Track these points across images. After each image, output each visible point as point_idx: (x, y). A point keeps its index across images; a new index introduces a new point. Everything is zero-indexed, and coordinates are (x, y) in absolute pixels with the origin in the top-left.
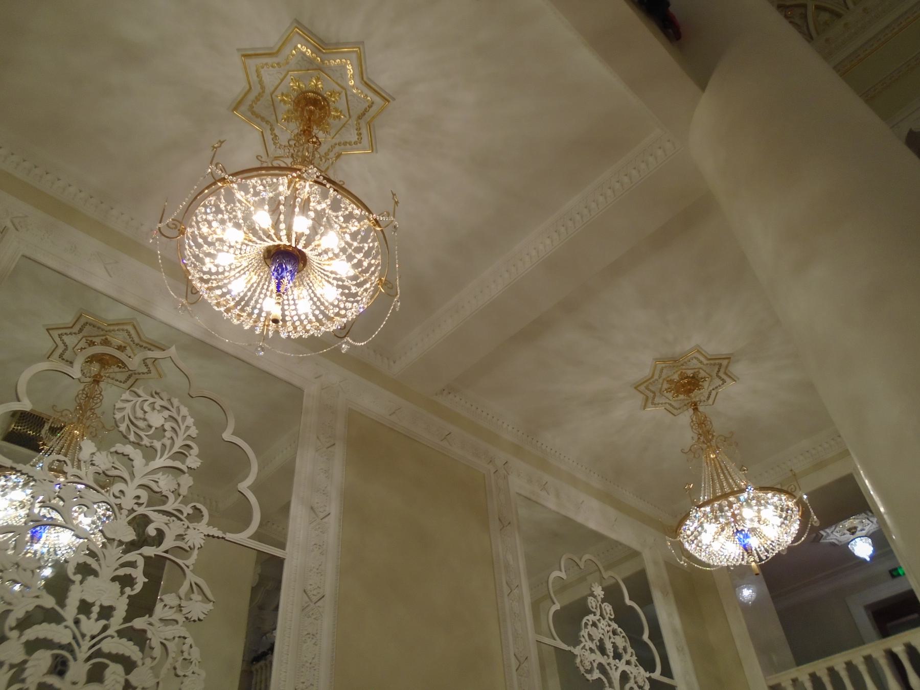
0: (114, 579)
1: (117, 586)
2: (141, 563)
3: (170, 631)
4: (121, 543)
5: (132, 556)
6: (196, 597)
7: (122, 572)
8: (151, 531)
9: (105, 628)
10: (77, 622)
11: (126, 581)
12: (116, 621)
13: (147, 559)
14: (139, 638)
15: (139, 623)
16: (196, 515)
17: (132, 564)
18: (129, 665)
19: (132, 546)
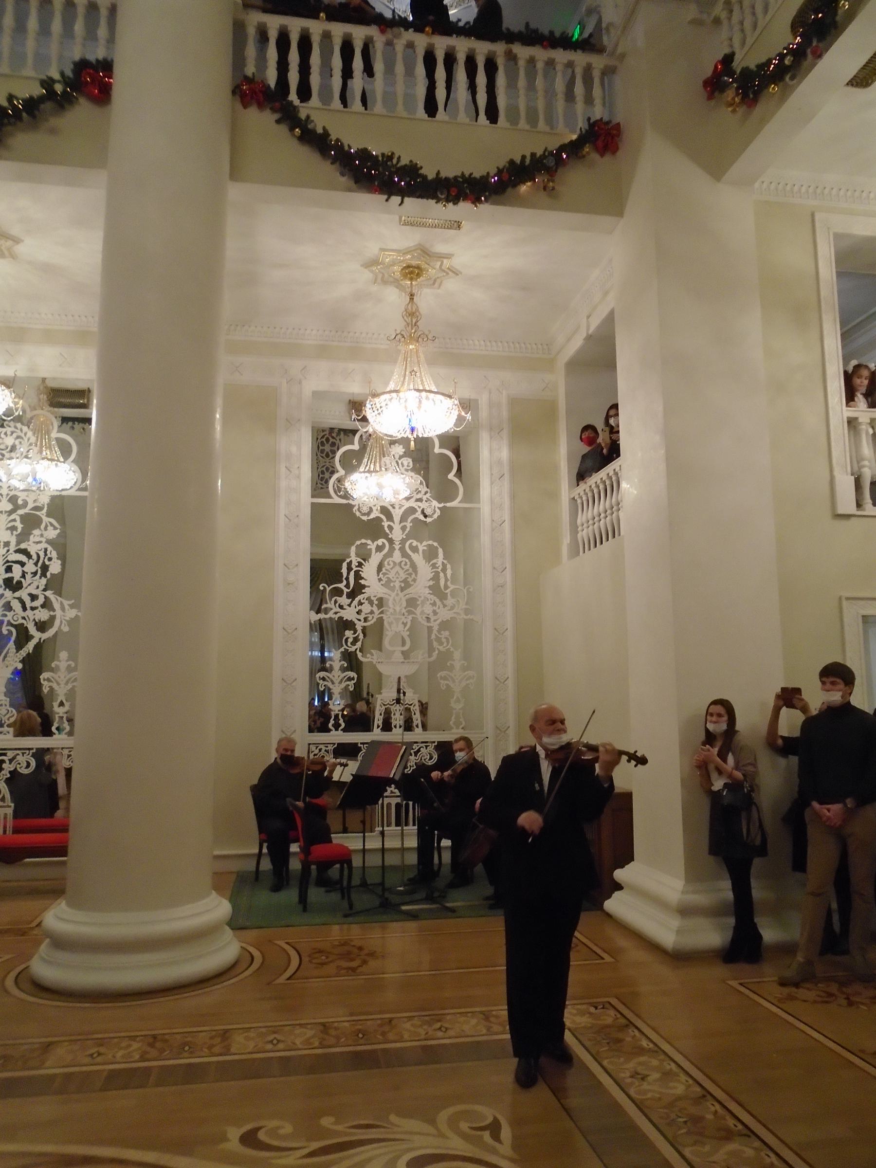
0: (7, 529)
1: (9, 532)
2: (18, 519)
3: (39, 546)
4: (6, 512)
5: (13, 517)
6: (50, 528)
7: (9, 525)
8: (20, 502)
9: (8, 551)
11: (13, 529)
12: (13, 547)
13: (21, 516)
14: (25, 552)
15: (23, 546)
17: (14, 520)
18: (22, 564)
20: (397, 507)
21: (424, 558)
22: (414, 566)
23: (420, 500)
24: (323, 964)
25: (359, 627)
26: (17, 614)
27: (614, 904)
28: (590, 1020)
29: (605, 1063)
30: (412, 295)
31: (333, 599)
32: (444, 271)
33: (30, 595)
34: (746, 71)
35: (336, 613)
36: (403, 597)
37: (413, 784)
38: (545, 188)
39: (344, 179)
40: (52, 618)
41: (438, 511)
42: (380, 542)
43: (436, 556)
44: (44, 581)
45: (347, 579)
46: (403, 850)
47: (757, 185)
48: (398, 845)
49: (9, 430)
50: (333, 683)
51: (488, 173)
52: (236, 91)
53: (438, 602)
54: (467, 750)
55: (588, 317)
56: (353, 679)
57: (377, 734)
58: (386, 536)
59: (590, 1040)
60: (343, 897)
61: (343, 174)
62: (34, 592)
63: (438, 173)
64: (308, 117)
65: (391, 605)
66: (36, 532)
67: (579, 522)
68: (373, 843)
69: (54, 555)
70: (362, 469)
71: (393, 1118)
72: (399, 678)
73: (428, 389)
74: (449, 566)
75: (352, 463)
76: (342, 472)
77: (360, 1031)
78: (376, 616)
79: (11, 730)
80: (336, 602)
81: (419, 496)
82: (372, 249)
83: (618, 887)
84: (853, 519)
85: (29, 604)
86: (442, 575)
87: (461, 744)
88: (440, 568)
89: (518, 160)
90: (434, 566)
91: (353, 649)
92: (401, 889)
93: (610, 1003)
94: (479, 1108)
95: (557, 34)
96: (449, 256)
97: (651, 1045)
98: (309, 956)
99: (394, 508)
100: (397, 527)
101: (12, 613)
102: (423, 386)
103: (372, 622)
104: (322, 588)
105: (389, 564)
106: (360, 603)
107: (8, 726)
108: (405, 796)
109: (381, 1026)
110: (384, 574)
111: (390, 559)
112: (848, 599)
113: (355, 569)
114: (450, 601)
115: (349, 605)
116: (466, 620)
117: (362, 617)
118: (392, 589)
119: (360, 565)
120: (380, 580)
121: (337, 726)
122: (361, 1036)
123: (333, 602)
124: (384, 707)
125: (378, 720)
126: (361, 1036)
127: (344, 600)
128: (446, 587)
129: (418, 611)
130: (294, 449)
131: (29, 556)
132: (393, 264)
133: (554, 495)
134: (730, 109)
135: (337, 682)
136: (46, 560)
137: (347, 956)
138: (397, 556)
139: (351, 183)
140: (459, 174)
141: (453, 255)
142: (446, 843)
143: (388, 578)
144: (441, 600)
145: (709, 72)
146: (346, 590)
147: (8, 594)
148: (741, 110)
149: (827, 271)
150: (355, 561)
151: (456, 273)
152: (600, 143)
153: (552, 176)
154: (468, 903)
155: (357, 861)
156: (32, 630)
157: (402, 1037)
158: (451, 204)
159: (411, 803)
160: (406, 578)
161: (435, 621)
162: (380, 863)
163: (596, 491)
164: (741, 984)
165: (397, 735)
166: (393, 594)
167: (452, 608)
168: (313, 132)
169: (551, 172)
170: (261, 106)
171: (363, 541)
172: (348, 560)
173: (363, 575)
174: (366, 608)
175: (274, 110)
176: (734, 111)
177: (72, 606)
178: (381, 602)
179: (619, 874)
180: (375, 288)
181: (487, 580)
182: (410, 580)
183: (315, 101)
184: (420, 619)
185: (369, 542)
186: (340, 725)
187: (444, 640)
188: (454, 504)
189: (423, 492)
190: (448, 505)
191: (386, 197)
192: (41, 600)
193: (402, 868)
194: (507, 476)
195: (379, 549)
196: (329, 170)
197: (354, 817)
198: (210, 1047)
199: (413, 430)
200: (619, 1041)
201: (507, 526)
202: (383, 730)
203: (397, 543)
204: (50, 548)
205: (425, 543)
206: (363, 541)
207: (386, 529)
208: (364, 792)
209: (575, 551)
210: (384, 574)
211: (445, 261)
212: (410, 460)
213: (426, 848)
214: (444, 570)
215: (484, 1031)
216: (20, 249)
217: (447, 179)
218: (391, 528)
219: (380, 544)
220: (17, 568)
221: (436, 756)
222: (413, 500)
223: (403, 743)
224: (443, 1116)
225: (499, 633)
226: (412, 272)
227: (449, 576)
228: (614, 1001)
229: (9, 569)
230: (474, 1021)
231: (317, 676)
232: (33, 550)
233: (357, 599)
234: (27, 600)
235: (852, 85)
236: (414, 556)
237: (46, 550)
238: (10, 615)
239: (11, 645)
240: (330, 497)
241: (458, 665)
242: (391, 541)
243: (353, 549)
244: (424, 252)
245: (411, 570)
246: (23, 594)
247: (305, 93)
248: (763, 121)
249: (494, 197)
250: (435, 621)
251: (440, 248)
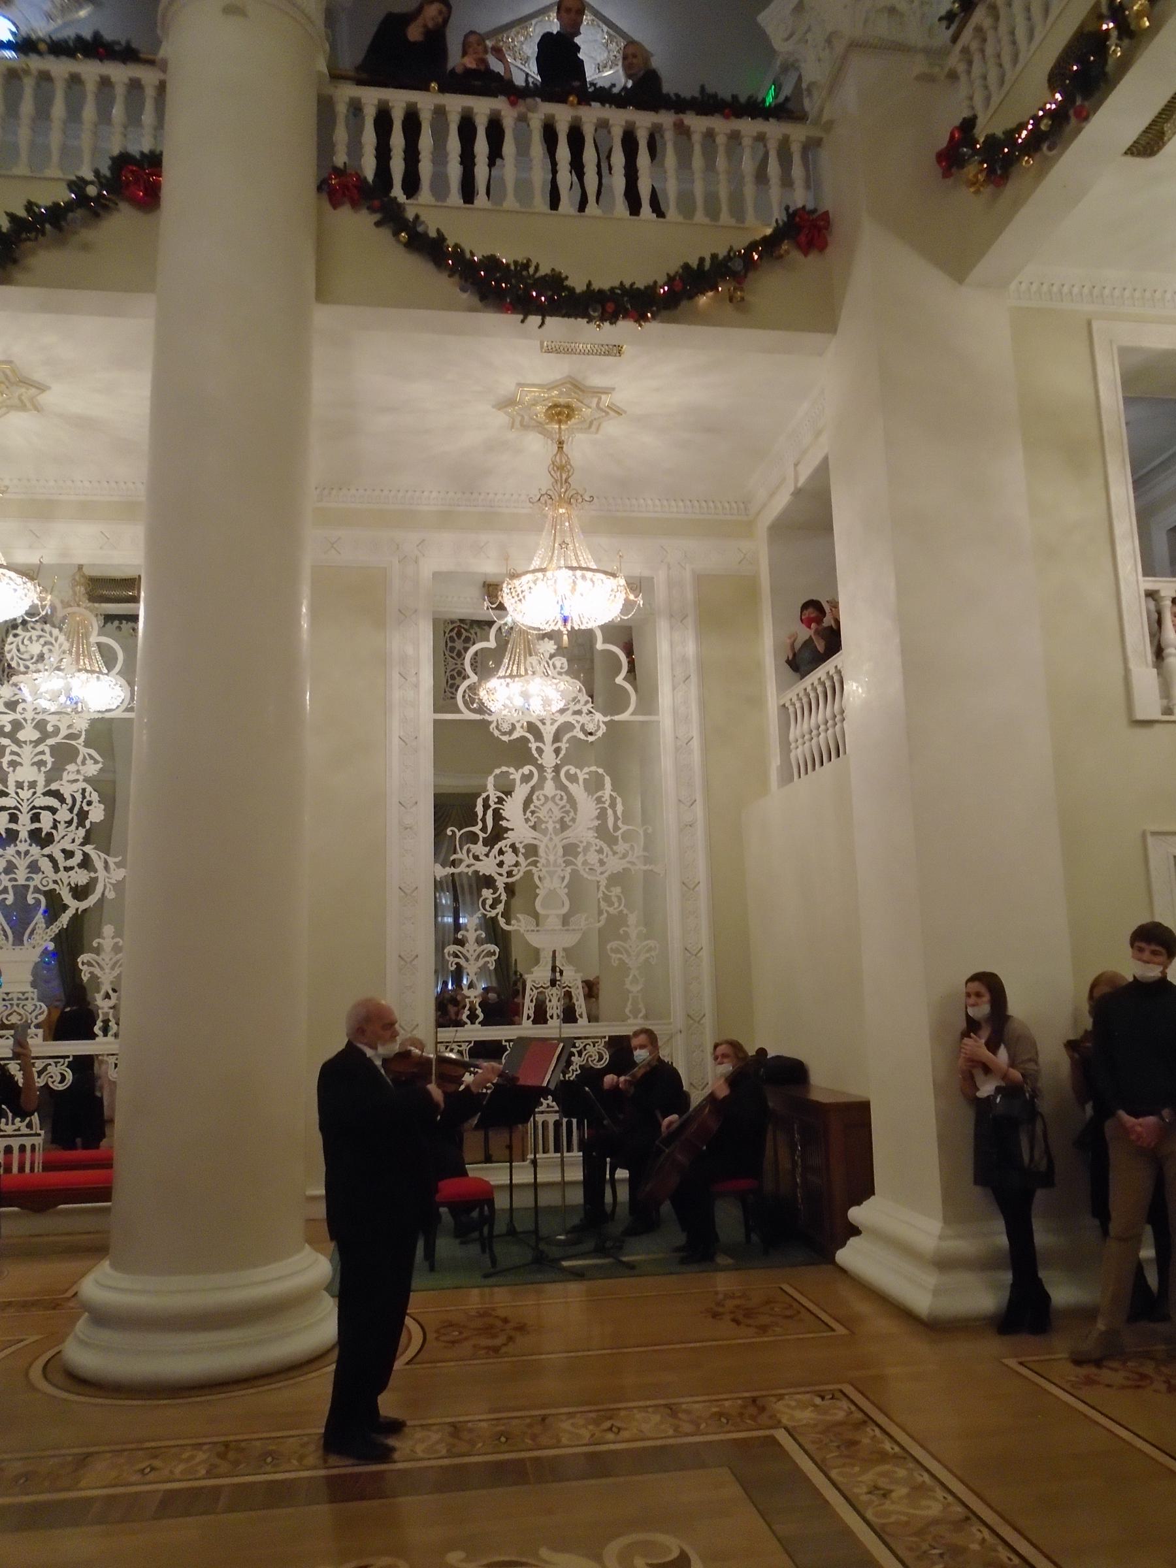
1: (35, 768)
2: (47, 750)
3: (75, 786)
4: (31, 742)
6: (89, 761)
7: (36, 759)
8: (50, 728)
9: (34, 793)
10: (17, 793)
12: (40, 789)
13: (52, 747)
15: (54, 787)
17: (42, 753)
18: (53, 811)
19: (37, 743)
20: (548, 722)
21: (586, 789)
22: (572, 800)
23: (579, 712)
24: (453, 1342)
25: (500, 883)
26: (46, 877)
27: (850, 1255)
28: (813, 1415)
29: (834, 1474)
30: (561, 443)
31: (465, 848)
32: (602, 410)
33: (63, 851)
34: (991, 140)
35: (468, 866)
36: (558, 842)
37: (578, 1096)
38: (731, 300)
39: (465, 296)
40: (92, 883)
41: (603, 727)
42: (526, 770)
43: (600, 786)
44: (81, 832)
45: (484, 820)
46: (564, 1184)
47: (1013, 286)
48: (556, 1177)
49: (34, 634)
50: (467, 960)
51: (655, 282)
52: (322, 186)
53: (606, 849)
54: (650, 1047)
55: (796, 465)
56: (494, 953)
57: (526, 1028)
58: (532, 761)
59: (813, 1442)
60: (484, 1251)
61: (463, 290)
62: (69, 847)
63: (589, 284)
64: (417, 217)
65: (541, 852)
66: (71, 767)
67: (792, 737)
68: (523, 1176)
69: (95, 797)
70: (501, 673)
71: (544, 1552)
72: (554, 952)
73: (584, 565)
74: (619, 800)
75: (486, 666)
76: (474, 678)
77: (502, 1434)
78: (523, 868)
79: (40, 1032)
80: (468, 851)
81: (577, 708)
82: (507, 384)
83: (855, 1231)
84: (1157, 727)
85: (62, 863)
86: (610, 812)
87: (642, 1038)
88: (608, 803)
89: (694, 264)
90: (599, 800)
91: (493, 913)
92: (562, 1237)
93: (841, 1391)
94: (660, 1537)
95: (743, 99)
96: (607, 391)
97: (897, 1449)
98: (437, 1331)
99: (544, 724)
100: (548, 749)
101: (40, 875)
102: (578, 561)
103: (517, 877)
104: (449, 833)
105: (539, 799)
106: (501, 852)
107: (37, 1026)
108: (566, 1111)
109: (530, 1426)
110: (533, 812)
111: (541, 792)
112: (1154, 834)
113: (494, 806)
114: (621, 847)
115: (487, 855)
116: (645, 871)
117: (504, 871)
118: (545, 832)
119: (500, 801)
120: (527, 820)
121: (473, 1017)
122: (503, 1439)
123: (465, 851)
124: (535, 992)
125: (529, 1008)
126: (503, 1439)
127: (479, 848)
128: (616, 828)
129: (580, 859)
130: (410, 650)
131: (62, 800)
132: (535, 403)
133: (756, 702)
134: (972, 190)
135: (472, 959)
136: (84, 805)
137: (488, 1330)
138: (549, 788)
139: (475, 300)
140: (617, 284)
141: (614, 389)
142: (622, 1174)
143: (538, 817)
144: (609, 846)
145: (943, 142)
146: (482, 835)
147: (35, 850)
148: (988, 190)
149: (1111, 398)
150: (493, 794)
151: (619, 412)
152: (803, 238)
153: (739, 283)
154: (651, 1256)
155: (501, 1201)
156: (67, 898)
157: (559, 1441)
158: (607, 324)
159: (574, 1121)
160: (562, 818)
161: (602, 873)
162: (531, 1204)
163: (812, 695)
164: (1021, 1363)
165: (554, 1028)
166: (545, 840)
167: (624, 856)
168: (425, 235)
169: (739, 279)
170: (355, 205)
171: (504, 769)
172: (484, 795)
173: (504, 814)
174: (510, 858)
175: (372, 210)
176: (977, 192)
177: (119, 865)
178: (532, 850)
179: (856, 1214)
180: (511, 435)
181: (669, 816)
182: (567, 819)
183: (425, 194)
184: (582, 872)
185: (512, 770)
186: (477, 1017)
187: (614, 899)
188: (624, 716)
189: (582, 702)
190: (616, 718)
191: (521, 317)
192: (78, 857)
193: (563, 1210)
194: (694, 679)
195: (526, 779)
196: (445, 285)
197: (498, 1139)
198: (301, 1458)
199: (565, 620)
200: (853, 1443)
201: (696, 744)
202: (534, 1022)
203: (549, 771)
204: (89, 789)
205: (586, 770)
206: (504, 769)
207: (534, 752)
208: (510, 1105)
209: (787, 777)
210: (533, 812)
211: (603, 397)
212: (564, 660)
213: (594, 1182)
214: (613, 805)
215: (671, 1432)
216: (44, 399)
217: (601, 291)
218: (540, 751)
219: (527, 772)
220: (46, 817)
221: (607, 1056)
222: (570, 712)
223: (560, 1040)
224: (613, 1548)
225: (688, 887)
226: (561, 412)
227: (619, 814)
228: (849, 1390)
229: (36, 818)
230: (656, 1418)
231: (446, 951)
232: (66, 792)
233: (497, 847)
234: (60, 857)
235: (1132, 154)
236: (572, 788)
237: (84, 790)
238: (37, 878)
239: (39, 918)
240: (459, 711)
241: (634, 933)
242: (541, 768)
243: (491, 779)
244: (576, 385)
245: (568, 807)
246: (55, 850)
247: (412, 185)
248: (1017, 204)
249: (664, 313)
250: (602, 873)
251: (596, 381)
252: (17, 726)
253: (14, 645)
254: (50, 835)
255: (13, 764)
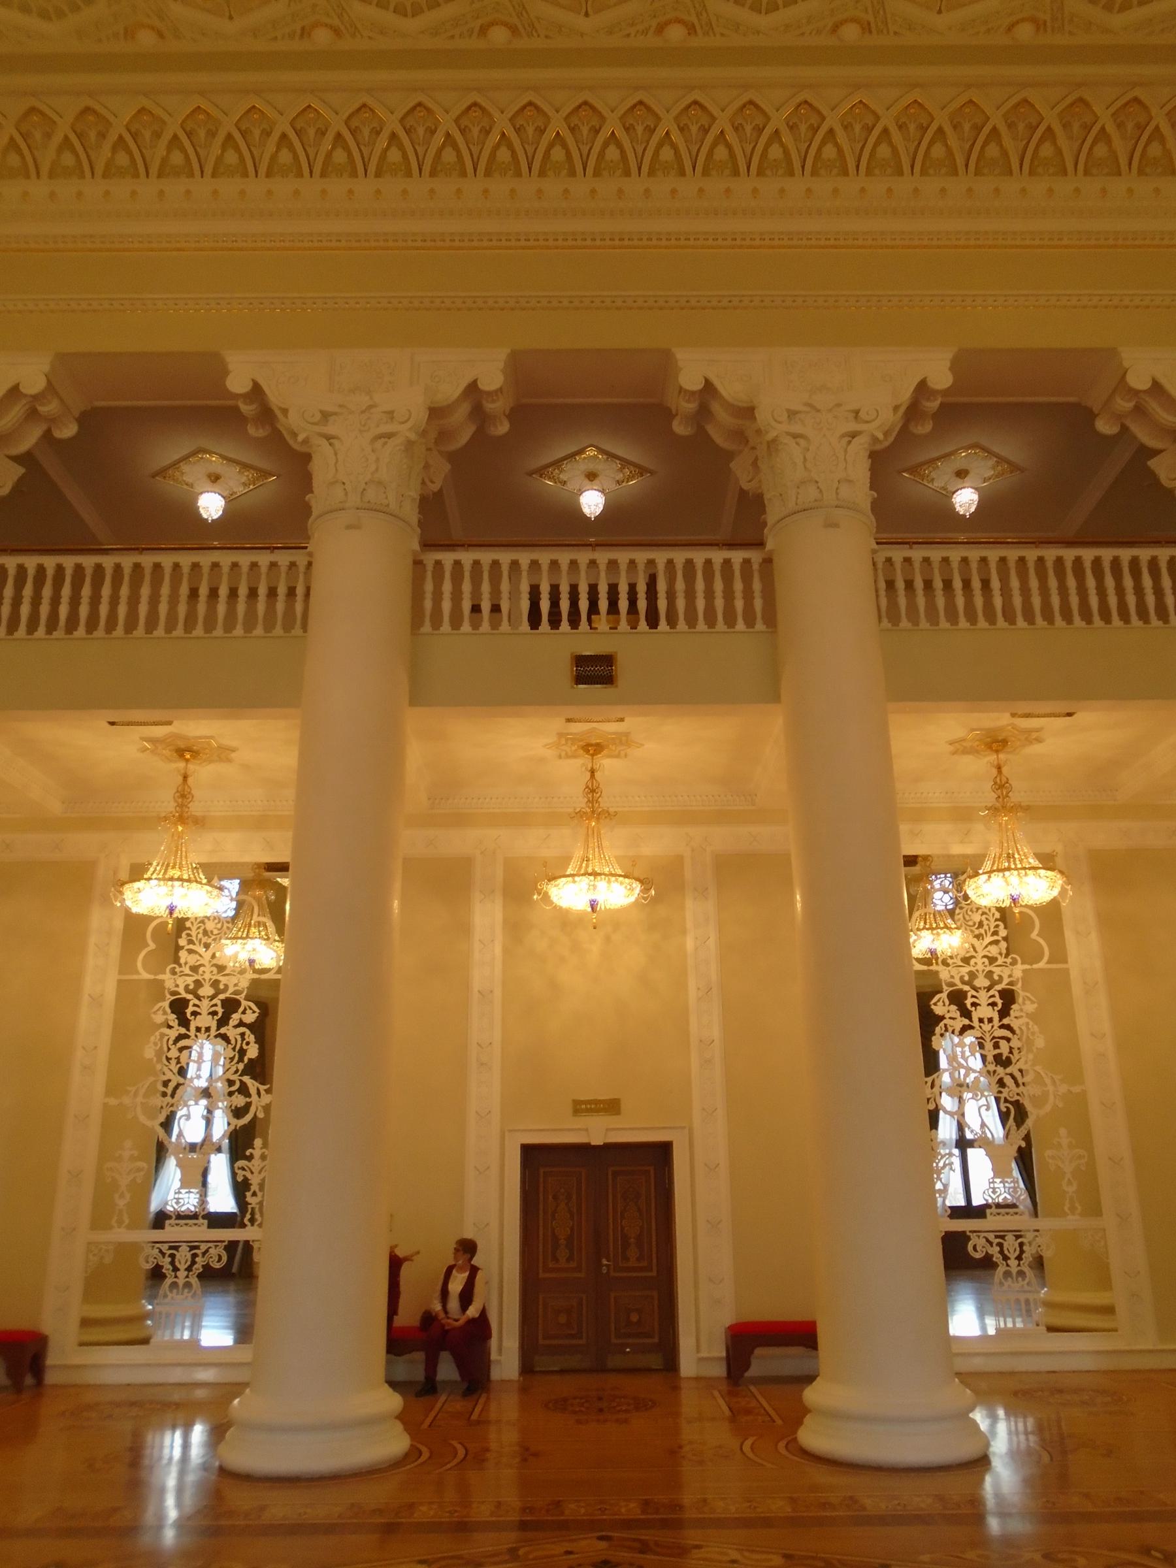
2: (997, 994)
3: (1020, 1021)
5: (991, 993)
6: (1028, 1002)
11: (993, 1004)
13: (999, 992)
14: (1008, 1027)
16: (1014, 963)
17: (993, 996)
18: (1008, 1040)
131: (1013, 1032)
147: (1000, 1069)
220: (1003, 1043)
229: (996, 1046)
237: (1028, 1024)
252: (973, 975)
253: (961, 916)
254: (1008, 1058)
255: (974, 1005)
